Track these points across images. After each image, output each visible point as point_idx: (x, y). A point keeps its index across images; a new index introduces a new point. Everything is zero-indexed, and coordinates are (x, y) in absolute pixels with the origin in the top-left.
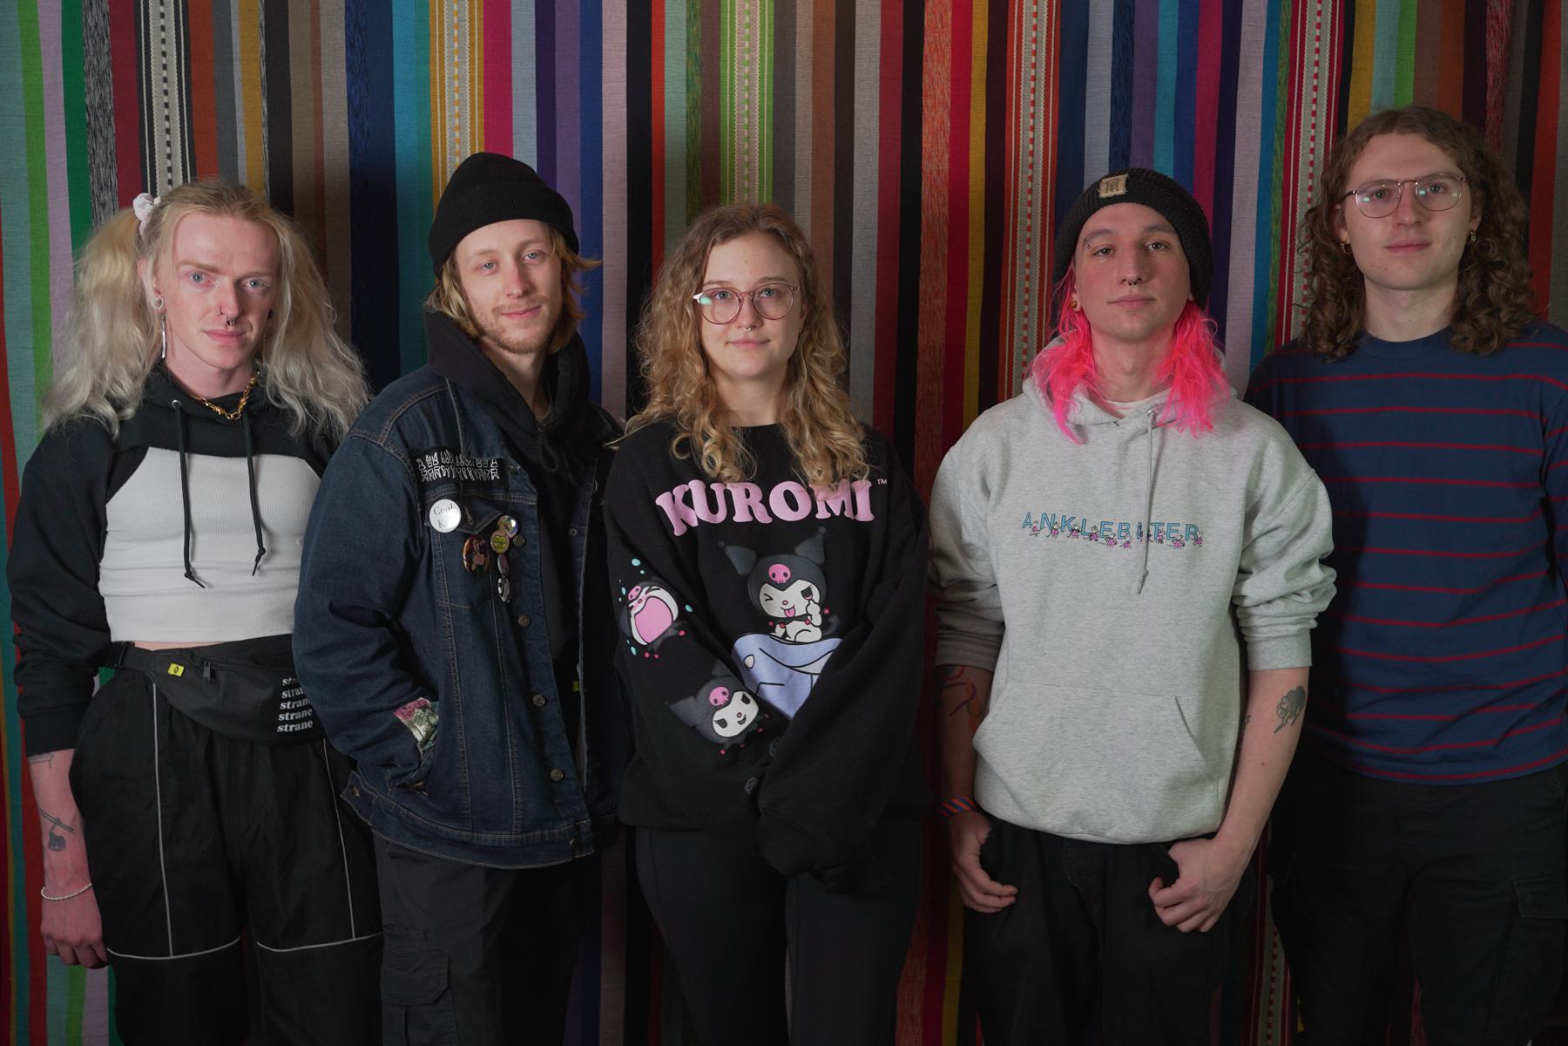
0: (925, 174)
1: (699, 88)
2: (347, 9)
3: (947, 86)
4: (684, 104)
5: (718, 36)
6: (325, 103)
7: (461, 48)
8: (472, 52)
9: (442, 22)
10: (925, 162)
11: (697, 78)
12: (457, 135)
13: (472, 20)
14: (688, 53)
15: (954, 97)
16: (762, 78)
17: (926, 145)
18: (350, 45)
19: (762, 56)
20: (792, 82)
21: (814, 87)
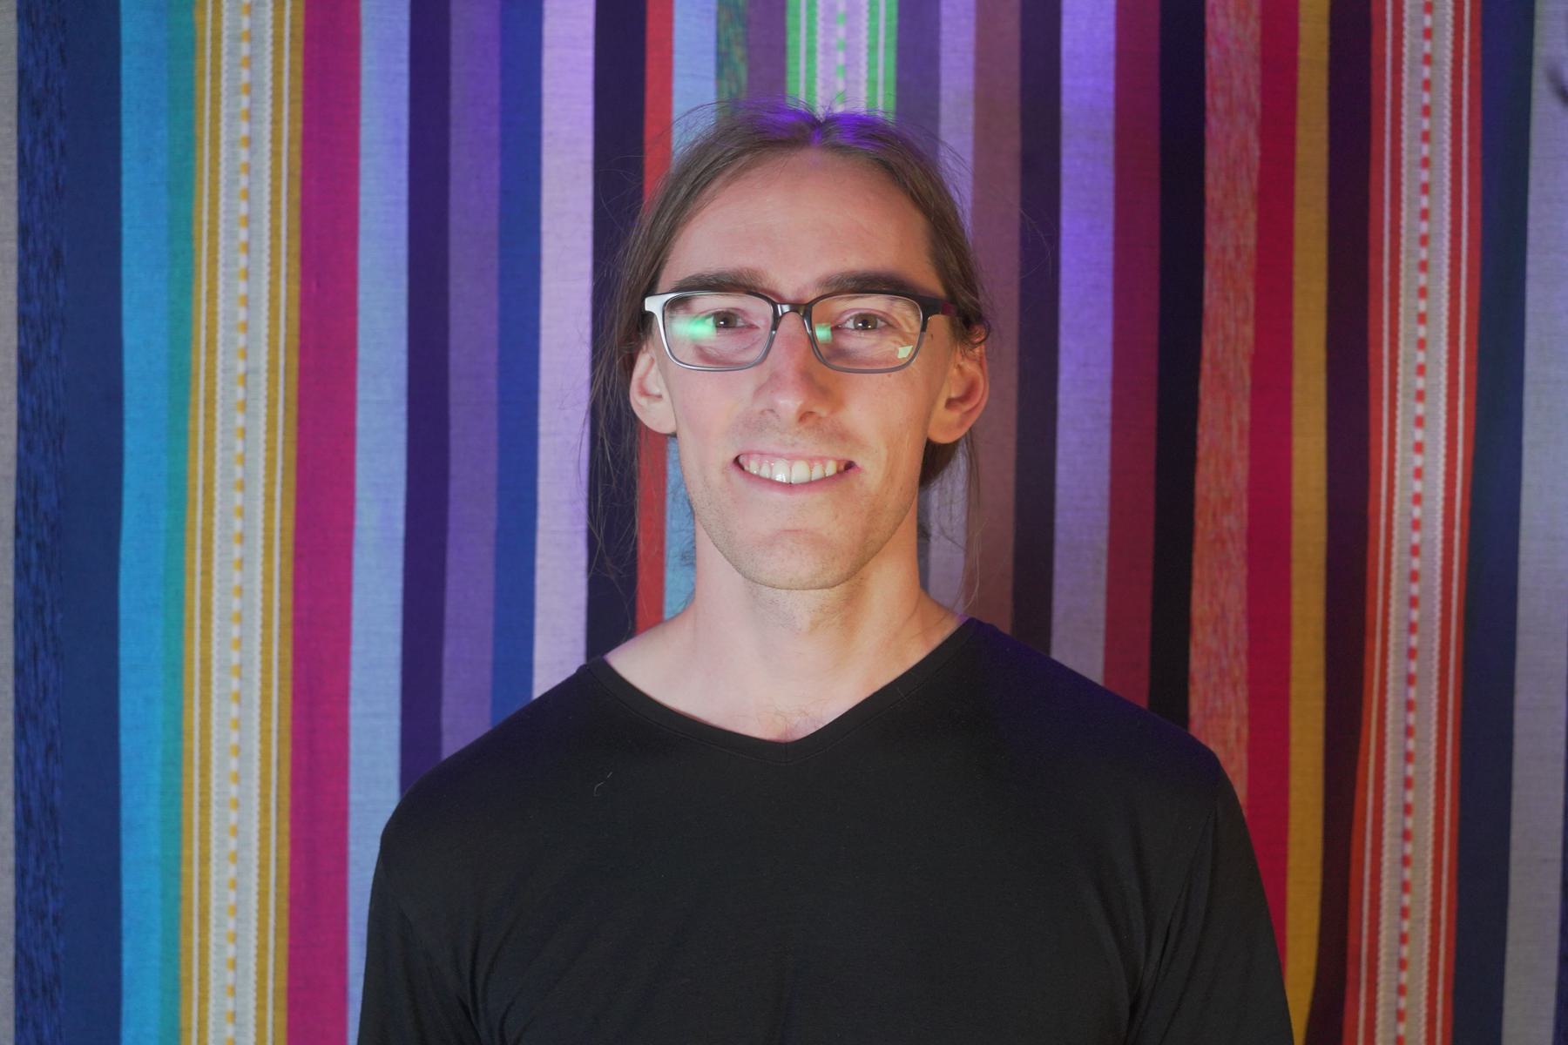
0: (1210, 258)
11: (738, 53)
12: (244, 155)
17: (1213, 193)
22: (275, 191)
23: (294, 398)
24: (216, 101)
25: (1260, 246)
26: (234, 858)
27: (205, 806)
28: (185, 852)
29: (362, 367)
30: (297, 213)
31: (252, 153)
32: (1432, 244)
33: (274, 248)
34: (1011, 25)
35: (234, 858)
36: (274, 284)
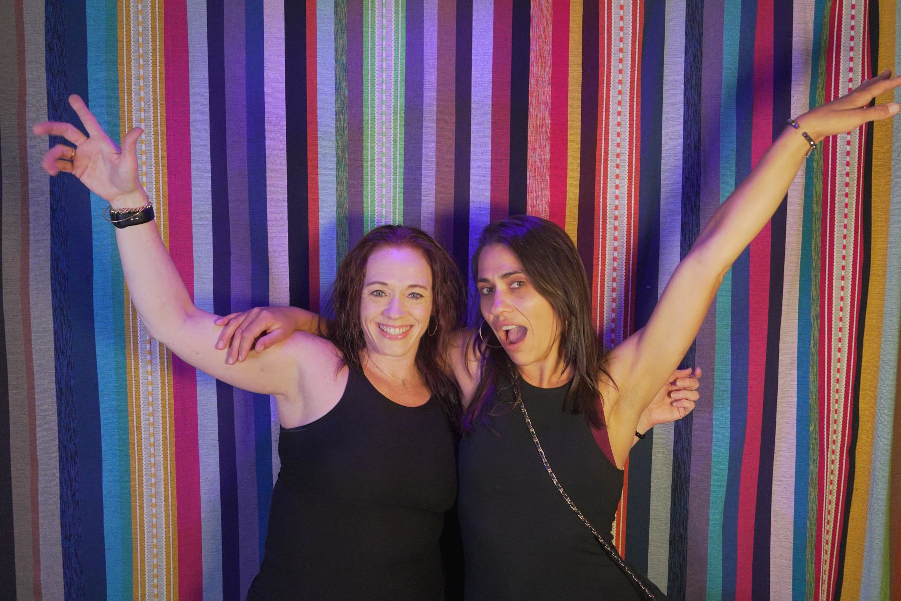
1: (346, 91)
2: (47, 18)
3: (548, 89)
4: (334, 105)
5: (362, 47)
6: (29, 98)
7: (145, 53)
8: (154, 56)
9: (129, 31)
10: (530, 153)
11: (344, 83)
13: (154, 28)
14: (337, 61)
15: (553, 99)
16: (396, 82)
18: (49, 48)
19: (396, 64)
20: (421, 85)
21: (438, 90)
22: (156, 141)
23: (167, 223)
24: (130, 103)
25: (552, 159)
26: (152, 404)
27: (137, 384)
28: (130, 403)
29: (193, 211)
30: (165, 149)
31: (146, 125)
32: (621, 157)
33: (157, 163)
34: (452, 70)
35: (152, 404)
36: (157, 178)
